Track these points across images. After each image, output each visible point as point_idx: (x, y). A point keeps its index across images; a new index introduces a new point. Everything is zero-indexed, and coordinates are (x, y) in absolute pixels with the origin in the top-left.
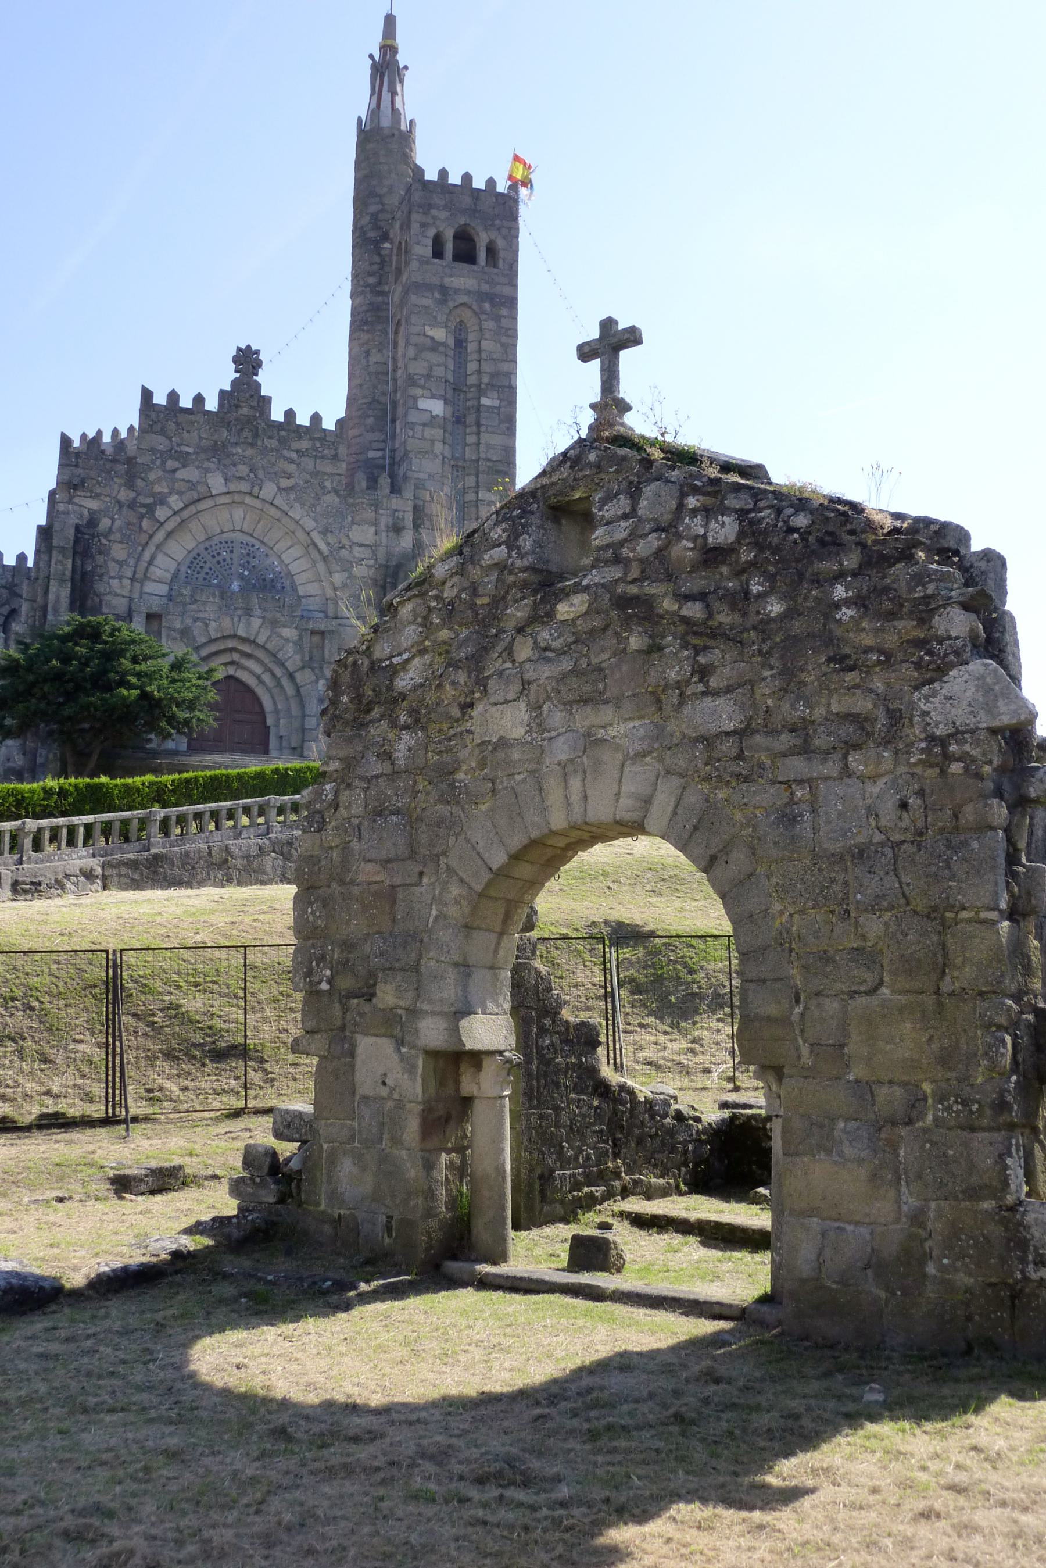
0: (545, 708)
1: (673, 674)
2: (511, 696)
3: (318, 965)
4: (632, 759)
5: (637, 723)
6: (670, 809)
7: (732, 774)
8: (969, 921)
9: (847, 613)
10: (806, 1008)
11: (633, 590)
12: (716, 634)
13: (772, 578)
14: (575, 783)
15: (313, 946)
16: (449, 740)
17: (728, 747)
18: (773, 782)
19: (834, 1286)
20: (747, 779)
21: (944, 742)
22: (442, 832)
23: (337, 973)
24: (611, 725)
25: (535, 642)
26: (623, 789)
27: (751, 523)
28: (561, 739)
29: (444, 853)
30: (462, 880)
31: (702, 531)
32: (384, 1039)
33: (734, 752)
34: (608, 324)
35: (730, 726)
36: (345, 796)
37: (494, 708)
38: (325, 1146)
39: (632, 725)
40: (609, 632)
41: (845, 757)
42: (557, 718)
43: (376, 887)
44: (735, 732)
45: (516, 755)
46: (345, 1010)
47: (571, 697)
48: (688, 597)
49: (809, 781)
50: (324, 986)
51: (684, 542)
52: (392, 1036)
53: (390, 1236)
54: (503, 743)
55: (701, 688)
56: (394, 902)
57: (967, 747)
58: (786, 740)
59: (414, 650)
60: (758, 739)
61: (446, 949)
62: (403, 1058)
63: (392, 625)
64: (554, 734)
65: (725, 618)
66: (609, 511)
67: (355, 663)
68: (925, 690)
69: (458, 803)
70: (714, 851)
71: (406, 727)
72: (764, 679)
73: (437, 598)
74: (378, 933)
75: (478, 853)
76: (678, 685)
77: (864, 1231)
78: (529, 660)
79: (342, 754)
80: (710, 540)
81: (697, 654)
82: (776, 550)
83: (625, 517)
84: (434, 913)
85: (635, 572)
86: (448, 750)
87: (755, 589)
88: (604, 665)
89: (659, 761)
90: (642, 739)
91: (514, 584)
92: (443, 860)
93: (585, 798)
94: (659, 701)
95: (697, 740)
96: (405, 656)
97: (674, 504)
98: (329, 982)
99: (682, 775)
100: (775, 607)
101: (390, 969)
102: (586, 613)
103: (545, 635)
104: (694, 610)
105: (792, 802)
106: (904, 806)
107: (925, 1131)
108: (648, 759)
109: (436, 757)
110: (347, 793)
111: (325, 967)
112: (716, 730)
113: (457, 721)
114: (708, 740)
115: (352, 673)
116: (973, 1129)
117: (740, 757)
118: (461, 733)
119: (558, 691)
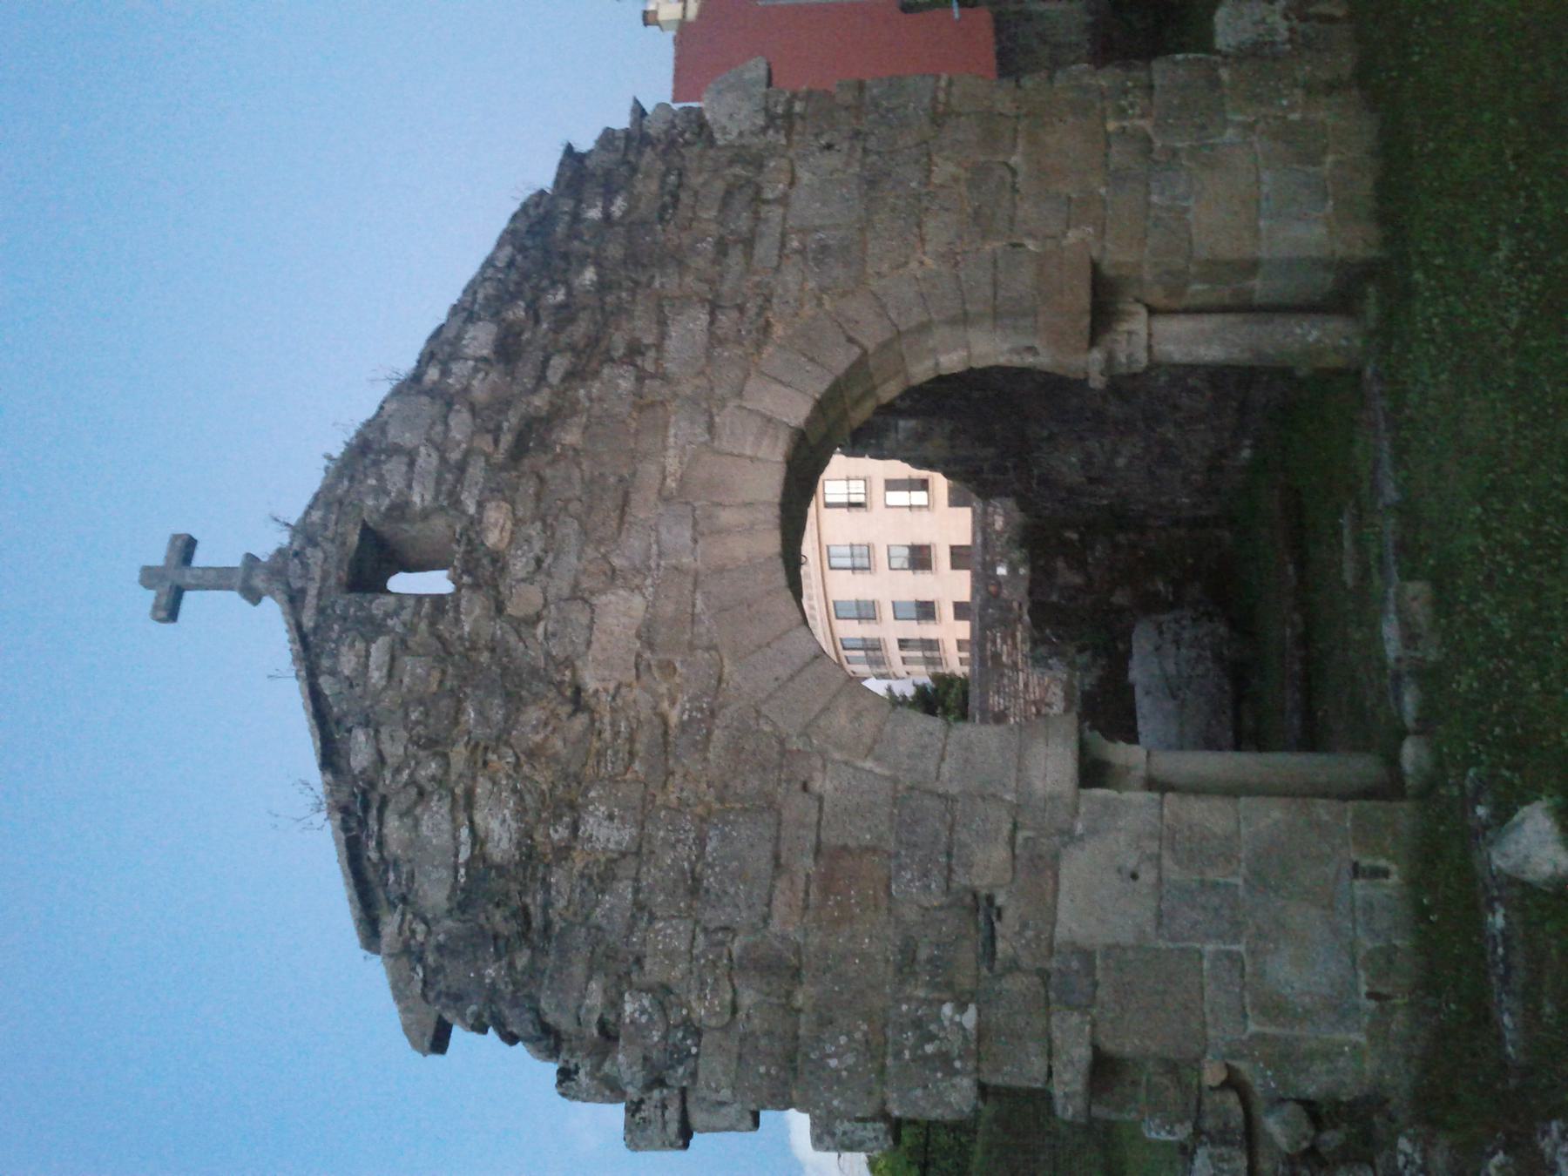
0: (617, 562)
1: (626, 385)
2: (585, 620)
3: (931, 1038)
4: (712, 439)
5: (672, 431)
6: (783, 389)
7: (759, 315)
8: (948, 94)
9: (619, 206)
10: (1030, 235)
11: (507, 439)
12: (594, 341)
13: (554, 283)
14: (726, 517)
15: (898, 1055)
16: (617, 734)
17: (726, 320)
18: (777, 269)
19: (1331, 203)
20: (768, 300)
21: (771, 118)
22: (749, 746)
23: (949, 985)
24: (664, 468)
25: (523, 580)
26: (748, 452)
27: (483, 307)
28: (664, 535)
29: (782, 742)
30: (825, 709)
31: (471, 363)
32: (1064, 872)
33: (735, 314)
34: (149, 577)
35: (704, 318)
36: (654, 970)
37: (595, 646)
38: (1253, 1028)
39: (671, 440)
40: (548, 473)
41: (766, 202)
42: (635, 543)
43: (813, 889)
44: (712, 313)
45: (669, 609)
46: (1013, 966)
47: (614, 524)
48: (541, 379)
49: (784, 235)
50: (970, 1018)
51: (475, 383)
52: (1056, 857)
53: (1385, 873)
54: (646, 635)
55: (652, 354)
56: (845, 848)
57: (782, 99)
58: (735, 257)
59: (462, 817)
60: (725, 288)
61: (926, 738)
62: (1093, 831)
63: (405, 869)
64: (655, 547)
65: (580, 330)
66: (395, 482)
67: (440, 948)
68: (717, 136)
69: (713, 714)
70: (842, 340)
71: (575, 828)
72: (662, 286)
73: (397, 771)
74: (888, 887)
75: (792, 678)
76: (640, 379)
77: (1266, 176)
78: (544, 591)
79: (578, 970)
80: (485, 352)
81: (612, 360)
82: (526, 277)
83: (412, 464)
84: (869, 764)
85: (485, 443)
86: (631, 740)
87: (561, 296)
88: (587, 475)
89: (724, 406)
90: (692, 422)
91: (432, 624)
92: (795, 744)
93: (747, 505)
94: (652, 405)
95: (709, 357)
96: (464, 833)
97: (424, 400)
98: (961, 1008)
99: (747, 376)
100: (589, 275)
101: (949, 855)
102: (513, 503)
103: (519, 566)
104: (559, 365)
105: (802, 252)
106: (829, 147)
107: (1156, 125)
108: (717, 419)
109: (637, 766)
110: (648, 964)
111: (938, 1018)
112: (705, 339)
113: (593, 721)
114: (715, 340)
115: (455, 954)
116: (1151, 87)
117: (741, 309)
118: (613, 710)
119: (601, 541)
